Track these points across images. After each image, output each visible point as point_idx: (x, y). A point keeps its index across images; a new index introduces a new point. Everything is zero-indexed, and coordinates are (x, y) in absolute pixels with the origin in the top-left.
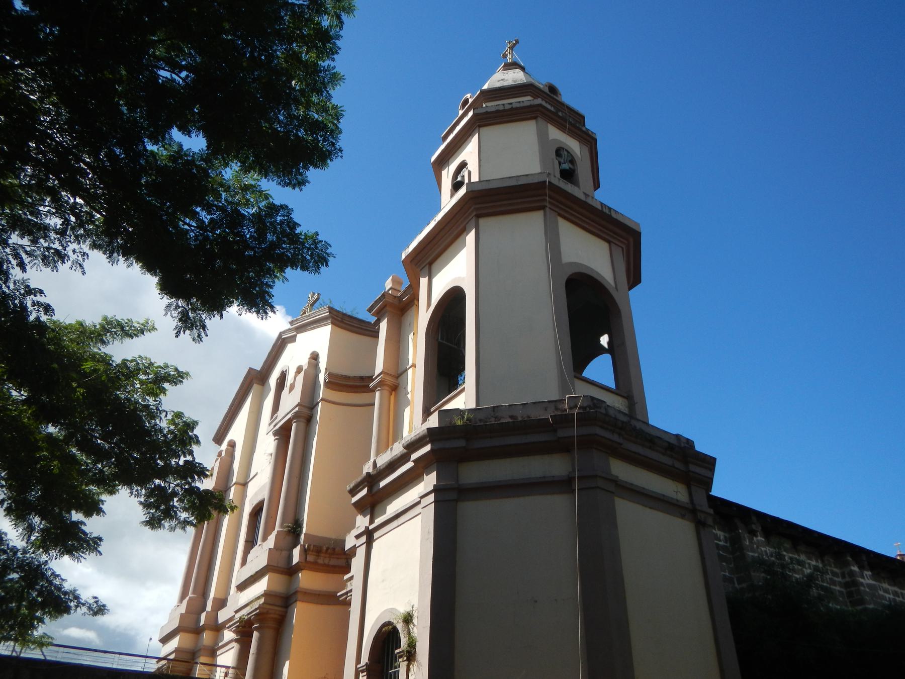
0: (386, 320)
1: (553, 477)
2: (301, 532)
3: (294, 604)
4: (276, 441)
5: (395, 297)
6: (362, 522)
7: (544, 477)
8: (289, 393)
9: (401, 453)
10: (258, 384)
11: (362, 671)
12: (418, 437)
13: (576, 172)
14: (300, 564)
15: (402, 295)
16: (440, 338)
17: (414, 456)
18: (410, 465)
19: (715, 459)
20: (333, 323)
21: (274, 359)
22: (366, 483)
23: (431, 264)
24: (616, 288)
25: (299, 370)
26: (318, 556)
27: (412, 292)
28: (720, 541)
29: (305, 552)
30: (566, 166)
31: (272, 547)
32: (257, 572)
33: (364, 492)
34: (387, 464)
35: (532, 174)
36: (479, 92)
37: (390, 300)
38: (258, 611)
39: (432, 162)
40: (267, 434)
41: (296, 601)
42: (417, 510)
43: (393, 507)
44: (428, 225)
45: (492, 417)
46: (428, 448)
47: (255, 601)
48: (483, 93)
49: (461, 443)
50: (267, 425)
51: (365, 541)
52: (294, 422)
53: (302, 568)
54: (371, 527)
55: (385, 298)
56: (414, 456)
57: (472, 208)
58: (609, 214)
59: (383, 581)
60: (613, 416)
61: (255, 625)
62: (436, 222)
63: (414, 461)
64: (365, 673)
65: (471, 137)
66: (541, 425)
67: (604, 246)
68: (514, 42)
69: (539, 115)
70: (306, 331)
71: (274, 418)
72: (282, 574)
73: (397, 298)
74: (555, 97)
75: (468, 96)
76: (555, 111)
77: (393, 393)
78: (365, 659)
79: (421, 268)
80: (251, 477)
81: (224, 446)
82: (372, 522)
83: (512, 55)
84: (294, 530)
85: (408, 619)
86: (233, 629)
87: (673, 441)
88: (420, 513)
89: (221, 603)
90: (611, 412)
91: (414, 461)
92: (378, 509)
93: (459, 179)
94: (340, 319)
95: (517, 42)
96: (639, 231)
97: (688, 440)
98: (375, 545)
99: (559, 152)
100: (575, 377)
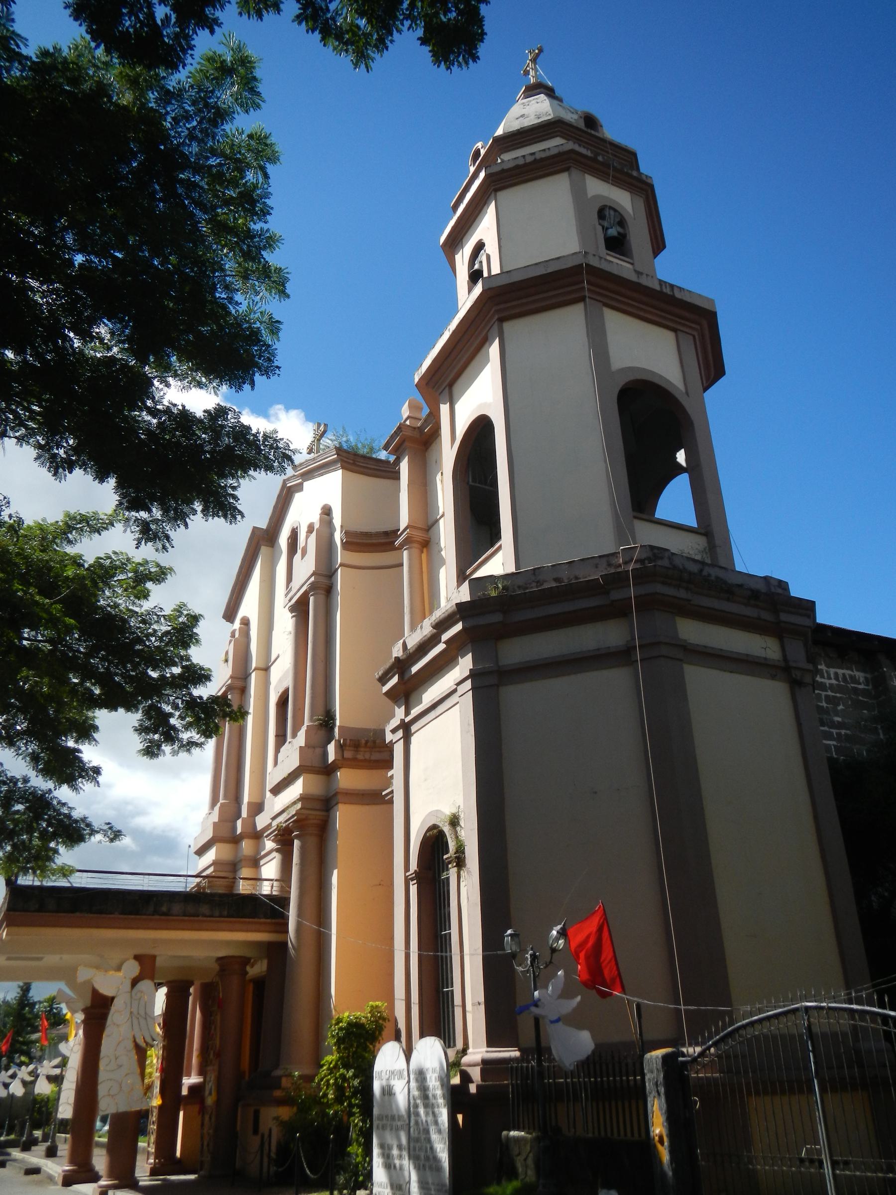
0: (406, 459)
1: (609, 647)
2: (334, 724)
3: (335, 808)
4: (294, 618)
5: (415, 428)
6: (400, 712)
7: (598, 649)
11: (412, 879)
12: (447, 614)
13: (628, 237)
14: (337, 762)
15: (423, 424)
16: (470, 480)
17: (446, 637)
18: (441, 647)
19: (813, 603)
20: (343, 468)
22: (396, 670)
23: (451, 385)
24: (687, 393)
25: (310, 529)
27: (434, 421)
28: (860, 684)
29: (340, 748)
30: (613, 232)
31: (304, 745)
32: (289, 774)
33: (395, 679)
34: (416, 646)
35: (564, 256)
36: (492, 140)
37: (408, 433)
38: (296, 817)
39: (441, 244)
41: (337, 804)
42: (454, 699)
43: (430, 695)
44: (441, 336)
45: (533, 581)
46: (459, 627)
48: (497, 140)
49: (497, 618)
50: (284, 595)
51: (402, 736)
52: (311, 595)
53: (340, 766)
54: (407, 720)
55: (401, 431)
56: (446, 637)
58: (672, 293)
59: (426, 780)
60: (681, 567)
62: (451, 332)
64: (415, 881)
65: (486, 207)
66: (591, 588)
67: (669, 336)
68: (537, 51)
69: (572, 165)
70: (313, 478)
74: (593, 132)
75: (479, 145)
76: (592, 155)
77: (425, 550)
78: (414, 866)
79: (440, 391)
80: (273, 659)
81: (237, 625)
82: (407, 713)
83: (536, 71)
84: (326, 722)
85: (454, 822)
86: (272, 838)
87: (761, 587)
88: (458, 703)
89: (258, 808)
90: (678, 562)
92: (413, 698)
93: (476, 267)
94: (351, 462)
95: (541, 50)
96: (712, 310)
97: (780, 581)
98: (414, 739)
99: (604, 212)
100: (635, 517)
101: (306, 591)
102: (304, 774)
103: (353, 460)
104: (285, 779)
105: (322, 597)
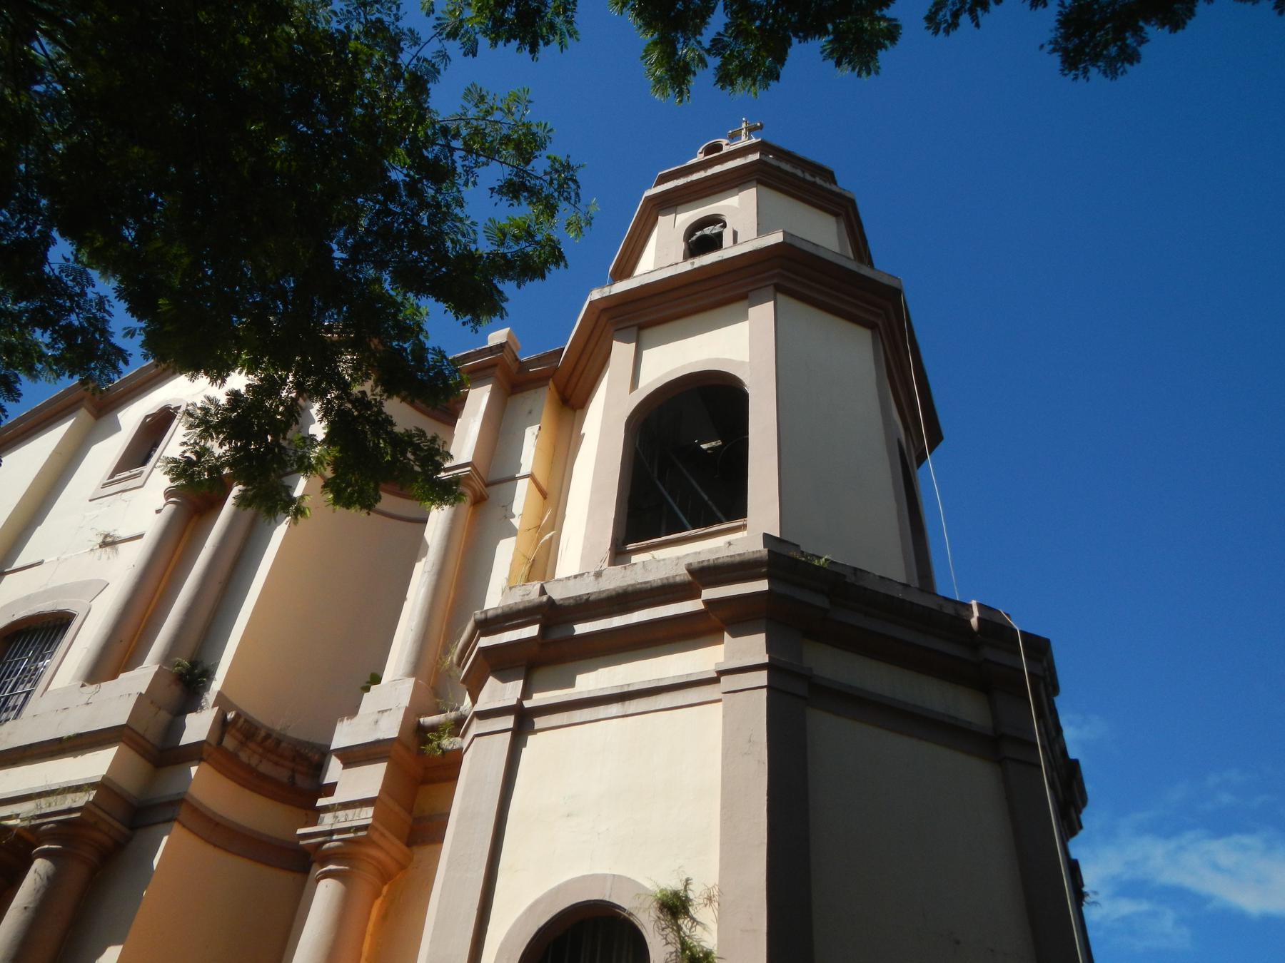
2: (206, 688)
5: (517, 360)
9: (665, 581)
10: (89, 412)
12: (738, 559)
21: (144, 384)
26: (242, 744)
29: (222, 725)
31: (143, 692)
33: (532, 631)
34: (614, 593)
37: (509, 360)
38: (77, 815)
40: (90, 500)
43: (590, 682)
46: (762, 585)
47: (58, 794)
49: (820, 601)
53: (205, 756)
55: (502, 351)
56: (709, 593)
57: (776, 271)
61: (46, 846)
63: (706, 602)
65: (736, 189)
68: (759, 124)
71: (116, 478)
72: (142, 755)
73: (517, 363)
75: (724, 142)
82: (526, 694)
91: (706, 602)
98: (534, 743)
102: (122, 744)
104: (60, 740)
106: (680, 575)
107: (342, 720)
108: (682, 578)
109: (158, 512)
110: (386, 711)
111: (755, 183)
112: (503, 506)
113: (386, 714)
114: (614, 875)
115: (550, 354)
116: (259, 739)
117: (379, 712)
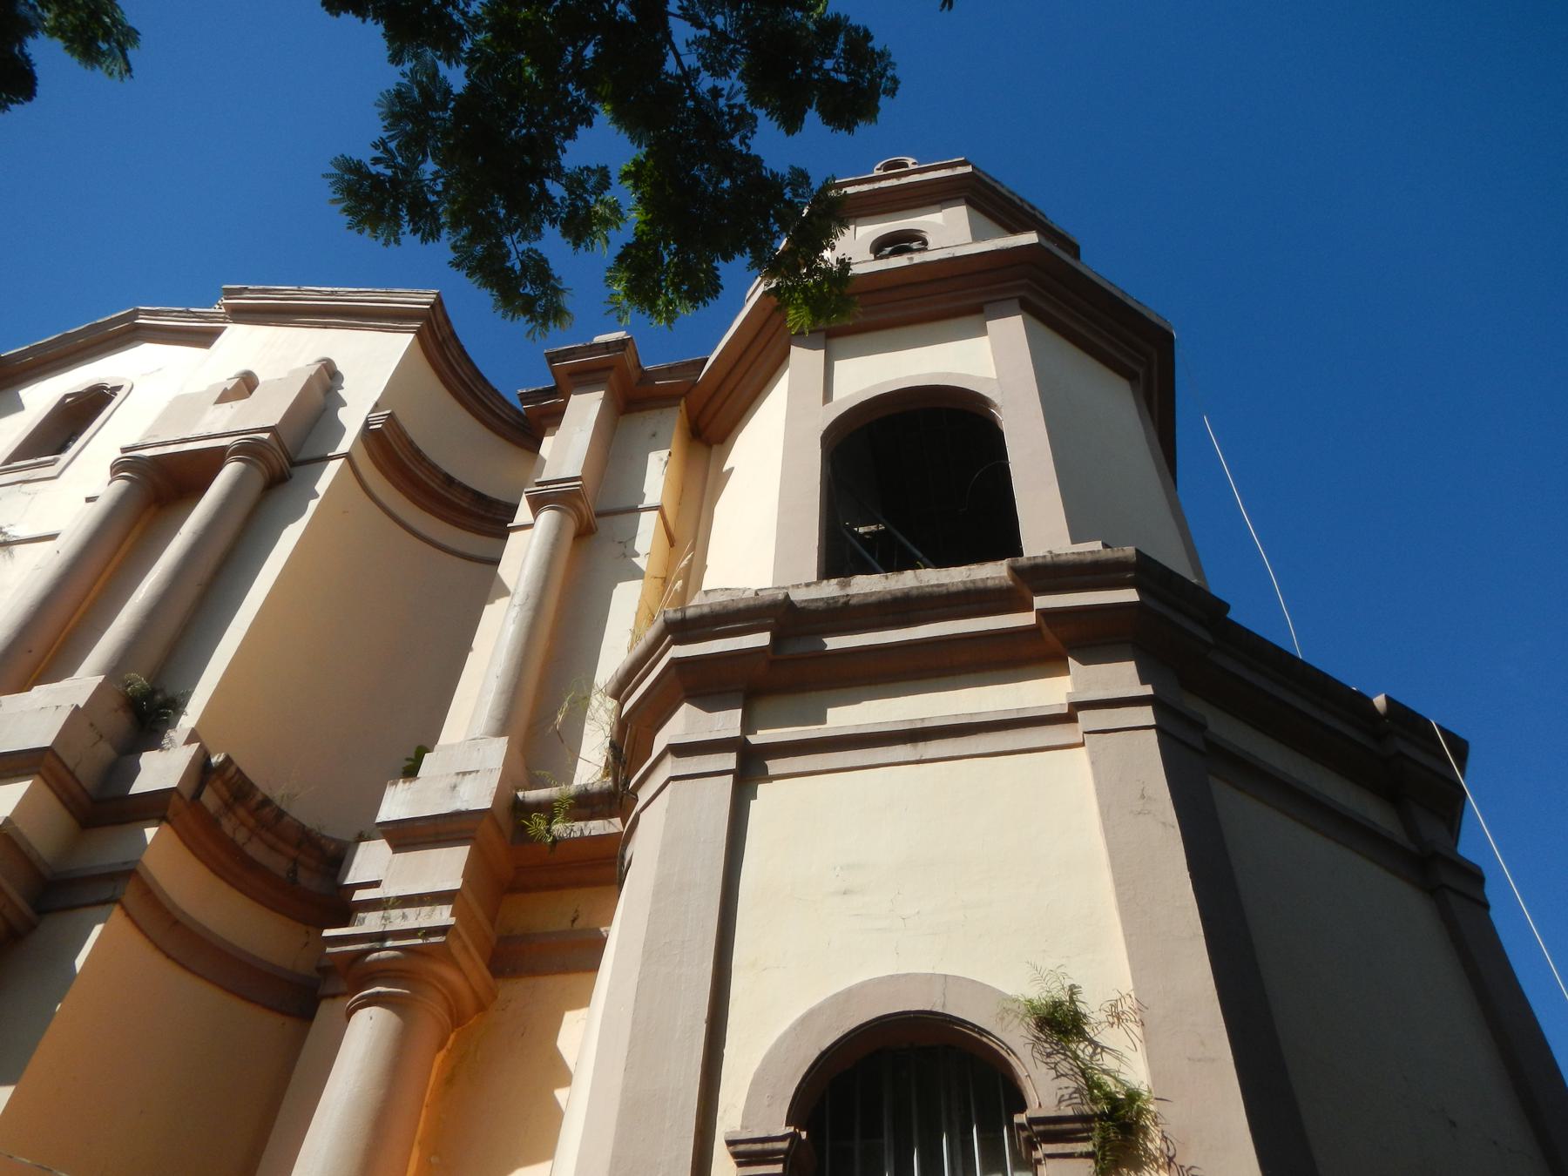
3: (98, 910)
5: (640, 366)
8: (216, 403)
20: (419, 334)
26: (228, 807)
29: (202, 770)
33: (762, 639)
34: (889, 597)
37: (630, 363)
43: (844, 718)
46: (1130, 595)
53: (169, 814)
56: (1041, 602)
65: (938, 206)
72: (65, 804)
75: (910, 161)
94: (440, 338)
101: (223, 449)
102: (37, 778)
103: (443, 338)
105: (258, 481)
106: (993, 578)
107: (396, 784)
108: (997, 582)
109: (89, 500)
110: (470, 773)
111: (963, 200)
112: (620, 542)
113: (468, 777)
114: (946, 976)
115: (687, 364)
116: (253, 804)
117: (458, 774)
